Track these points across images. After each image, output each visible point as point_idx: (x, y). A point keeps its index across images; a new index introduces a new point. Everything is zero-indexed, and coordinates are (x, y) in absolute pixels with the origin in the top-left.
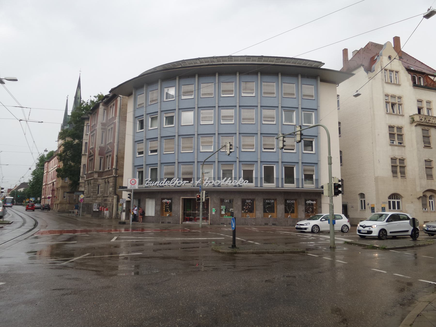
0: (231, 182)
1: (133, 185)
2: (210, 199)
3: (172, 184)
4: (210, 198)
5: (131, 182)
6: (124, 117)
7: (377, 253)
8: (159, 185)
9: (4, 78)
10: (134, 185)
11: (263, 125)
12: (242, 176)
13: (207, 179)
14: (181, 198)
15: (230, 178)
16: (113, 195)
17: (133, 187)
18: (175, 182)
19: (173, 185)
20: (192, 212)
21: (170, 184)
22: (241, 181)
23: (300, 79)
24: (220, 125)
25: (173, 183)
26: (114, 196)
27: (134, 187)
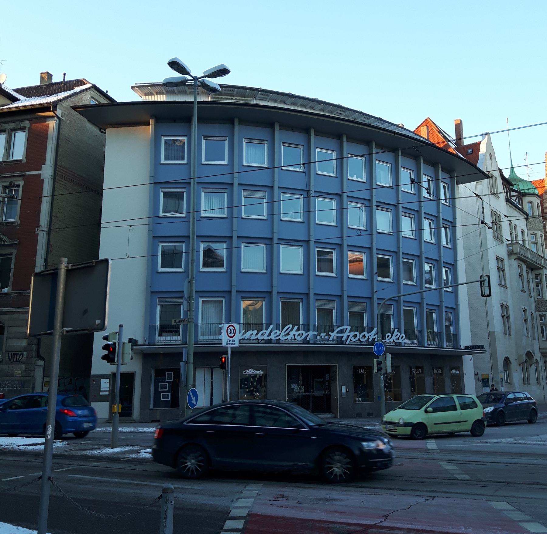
0: (257, 334)
1: (231, 339)
2: (337, 367)
3: (286, 338)
4: (338, 365)
5: (229, 332)
6: (62, 168)
7: (366, 450)
8: (256, 338)
9: (203, 75)
10: (233, 338)
11: (282, 222)
12: (301, 325)
13: (348, 330)
14: (286, 366)
15: (296, 327)
16: (35, 357)
17: (231, 342)
18: (292, 333)
19: (287, 339)
20: (393, 389)
21: (281, 337)
22: (397, 335)
23: (236, 129)
24: (281, 221)
25: (288, 334)
26: (36, 361)
27: (233, 343)
